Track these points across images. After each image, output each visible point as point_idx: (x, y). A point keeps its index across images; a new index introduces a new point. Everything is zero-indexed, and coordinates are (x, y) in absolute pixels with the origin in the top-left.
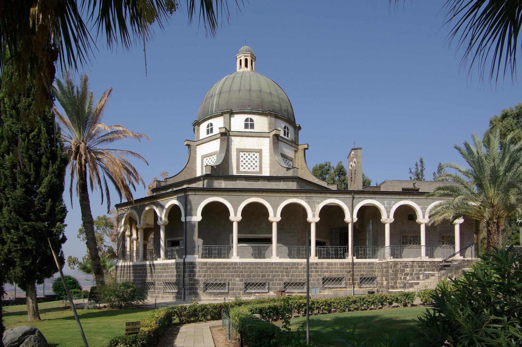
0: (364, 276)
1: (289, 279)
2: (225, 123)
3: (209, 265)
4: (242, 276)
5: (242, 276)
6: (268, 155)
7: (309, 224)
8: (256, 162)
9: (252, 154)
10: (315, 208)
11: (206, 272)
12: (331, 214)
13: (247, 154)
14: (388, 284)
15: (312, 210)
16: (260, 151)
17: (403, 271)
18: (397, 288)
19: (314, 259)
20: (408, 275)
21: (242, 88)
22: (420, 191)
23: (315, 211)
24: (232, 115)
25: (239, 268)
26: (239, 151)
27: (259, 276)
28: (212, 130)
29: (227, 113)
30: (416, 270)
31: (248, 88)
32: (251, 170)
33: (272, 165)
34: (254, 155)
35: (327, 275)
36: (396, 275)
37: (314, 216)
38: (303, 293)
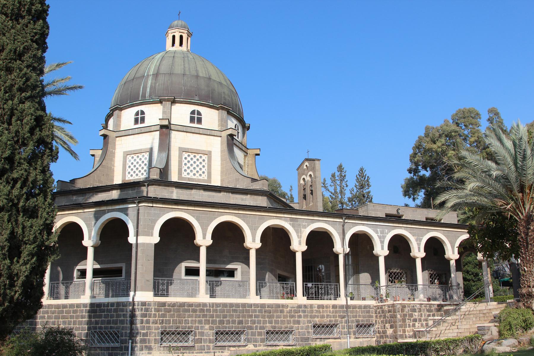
0: (361, 323)
1: (272, 327)
2: (164, 113)
3: (169, 305)
4: (214, 322)
5: (214, 322)
6: (219, 159)
7: (294, 254)
8: (204, 166)
9: (198, 156)
10: (301, 233)
11: (164, 316)
12: (319, 241)
13: (192, 156)
14: (395, 332)
15: (298, 236)
16: (209, 154)
17: (411, 315)
18: (406, 337)
19: (300, 299)
20: (416, 321)
22: (403, 218)
23: (301, 238)
25: (209, 311)
26: (182, 150)
27: (233, 322)
29: (168, 100)
30: (425, 315)
32: (197, 176)
33: (223, 173)
34: (201, 157)
35: (317, 320)
36: (404, 320)
37: (300, 243)
38: (289, 345)
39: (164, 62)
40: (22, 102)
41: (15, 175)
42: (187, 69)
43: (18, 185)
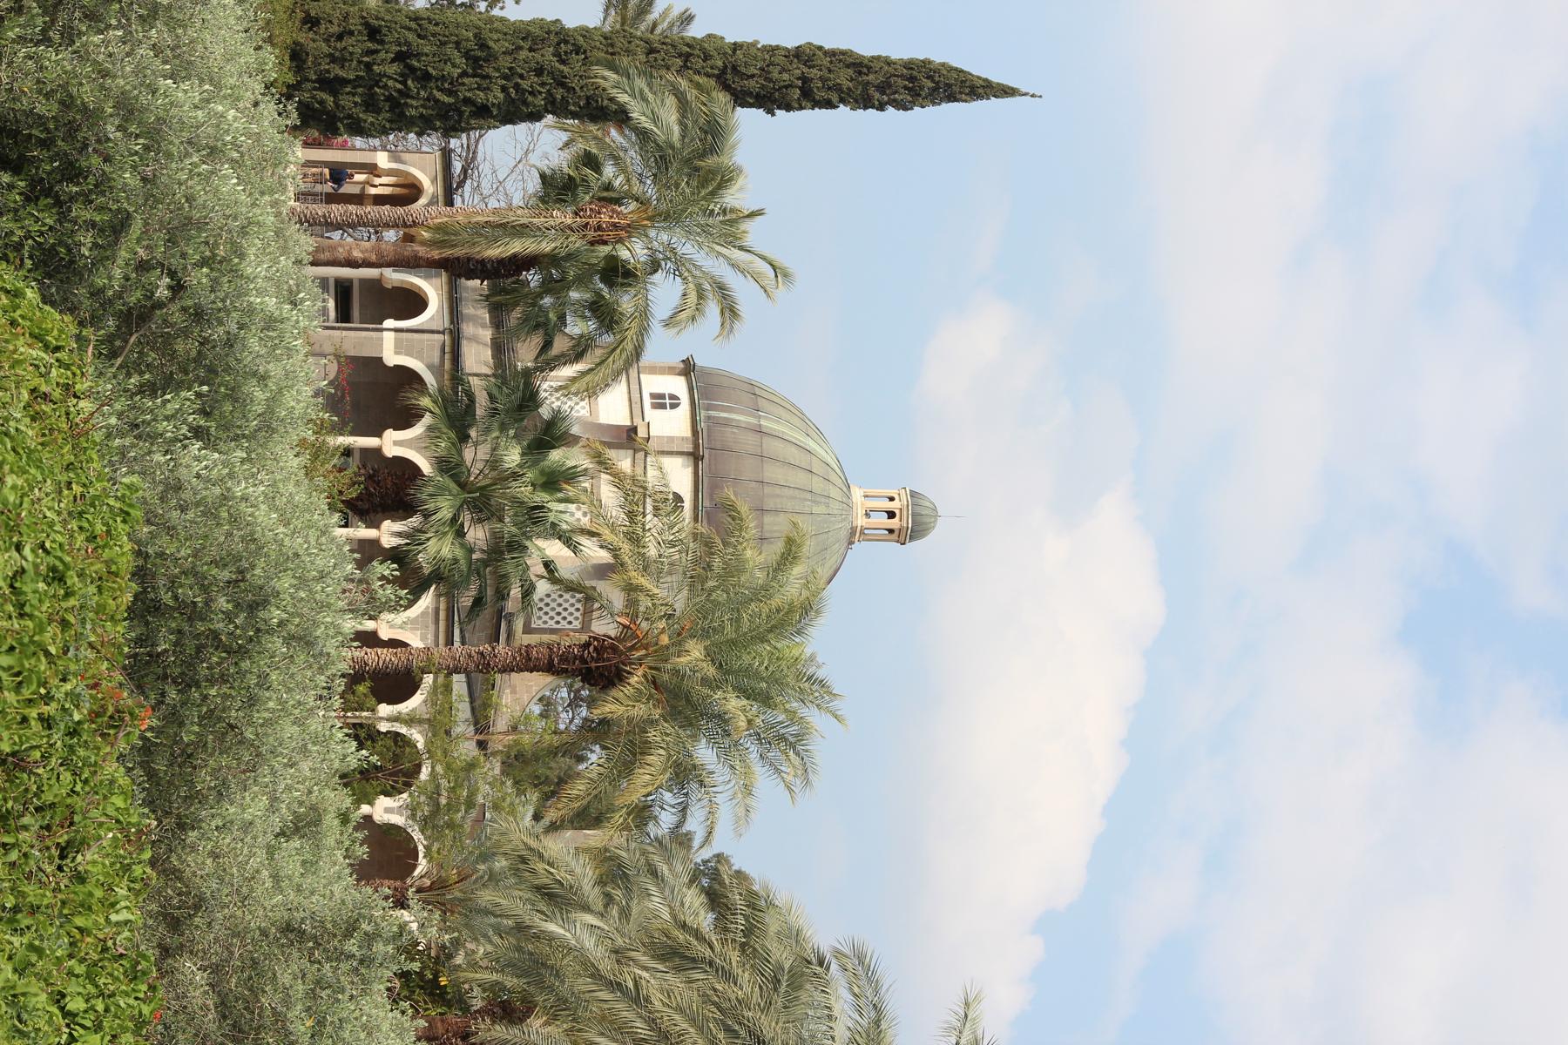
21: (767, 490)
24: (691, 459)
28: (663, 406)
29: (696, 446)
31: (770, 504)
39: (793, 449)
40: (504, 89)
41: (409, 82)
42: (777, 491)
43: (399, 86)
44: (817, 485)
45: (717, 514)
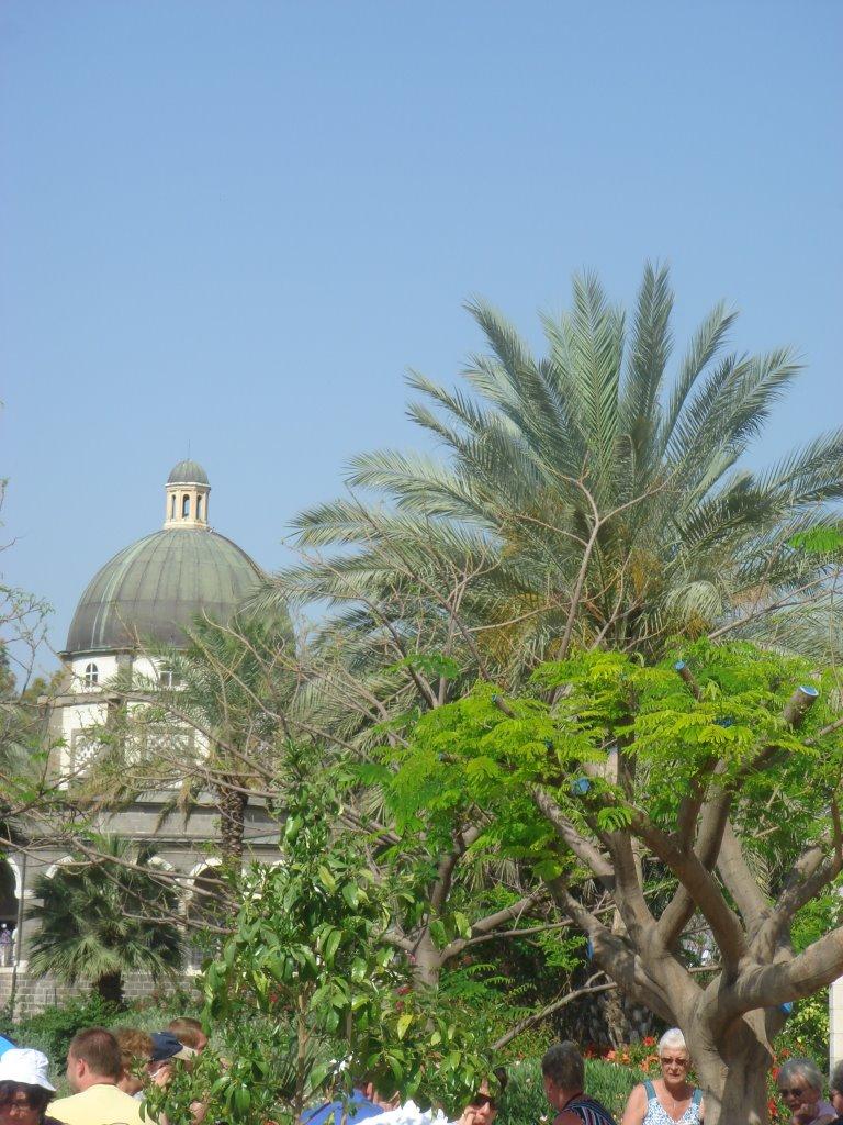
21: (162, 597)
28: (95, 677)
44: (159, 558)
45: (159, 640)
